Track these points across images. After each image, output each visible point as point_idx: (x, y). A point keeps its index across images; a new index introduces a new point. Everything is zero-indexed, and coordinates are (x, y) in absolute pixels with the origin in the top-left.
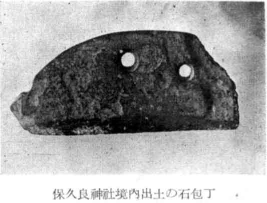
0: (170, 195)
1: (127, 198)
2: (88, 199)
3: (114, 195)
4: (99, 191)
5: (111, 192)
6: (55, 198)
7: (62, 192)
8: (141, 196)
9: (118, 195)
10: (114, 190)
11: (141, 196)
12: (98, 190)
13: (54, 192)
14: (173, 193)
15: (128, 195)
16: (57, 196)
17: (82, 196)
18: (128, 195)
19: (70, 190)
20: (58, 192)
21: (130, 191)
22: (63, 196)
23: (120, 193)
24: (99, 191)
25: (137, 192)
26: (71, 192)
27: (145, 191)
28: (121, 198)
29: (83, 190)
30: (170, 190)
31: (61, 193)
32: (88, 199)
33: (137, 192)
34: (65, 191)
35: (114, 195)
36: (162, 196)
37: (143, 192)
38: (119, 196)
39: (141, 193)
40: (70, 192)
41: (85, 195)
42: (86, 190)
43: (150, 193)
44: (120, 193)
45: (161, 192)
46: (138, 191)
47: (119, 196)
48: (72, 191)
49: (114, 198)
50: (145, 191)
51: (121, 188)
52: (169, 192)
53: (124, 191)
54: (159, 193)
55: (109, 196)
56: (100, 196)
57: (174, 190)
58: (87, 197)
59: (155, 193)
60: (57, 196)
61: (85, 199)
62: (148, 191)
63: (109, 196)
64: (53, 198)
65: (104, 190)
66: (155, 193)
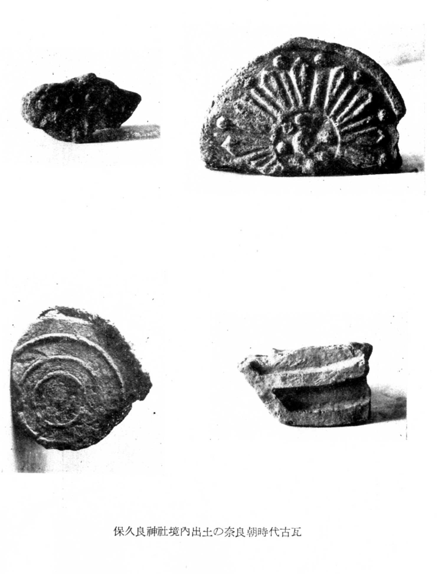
0: (218, 533)
1: (179, 535)
2: (144, 536)
3: (167, 532)
4: (155, 529)
5: (165, 530)
6: (116, 535)
7: (122, 529)
8: (191, 534)
9: (171, 532)
10: (168, 528)
11: (191, 534)
12: (154, 528)
13: (115, 529)
14: (220, 531)
15: (179, 532)
16: (117, 533)
17: (139, 533)
18: (179, 532)
19: (129, 527)
20: (119, 529)
21: (182, 529)
22: (122, 532)
23: (172, 531)
24: (155, 529)
25: (188, 530)
26: (130, 529)
27: (195, 529)
28: (173, 535)
29: (140, 527)
30: (217, 529)
31: (121, 530)
32: (144, 536)
33: (188, 530)
34: (125, 529)
35: (167, 532)
36: (210, 534)
37: (194, 531)
38: (172, 534)
39: (191, 531)
40: (129, 529)
41: (142, 532)
42: (143, 528)
43: (199, 531)
44: (172, 531)
45: (209, 530)
46: (189, 529)
47: (172, 534)
48: (131, 529)
49: (167, 535)
50: (195, 529)
51: (173, 527)
52: (216, 530)
53: (176, 528)
54: (207, 531)
55: (163, 533)
56: (155, 533)
57: (219, 528)
58: (143, 534)
59: (204, 531)
60: (117, 533)
61: (142, 535)
62: (198, 529)
63: (163, 533)
64: (114, 534)
65: (158, 527)
66: (204, 531)
